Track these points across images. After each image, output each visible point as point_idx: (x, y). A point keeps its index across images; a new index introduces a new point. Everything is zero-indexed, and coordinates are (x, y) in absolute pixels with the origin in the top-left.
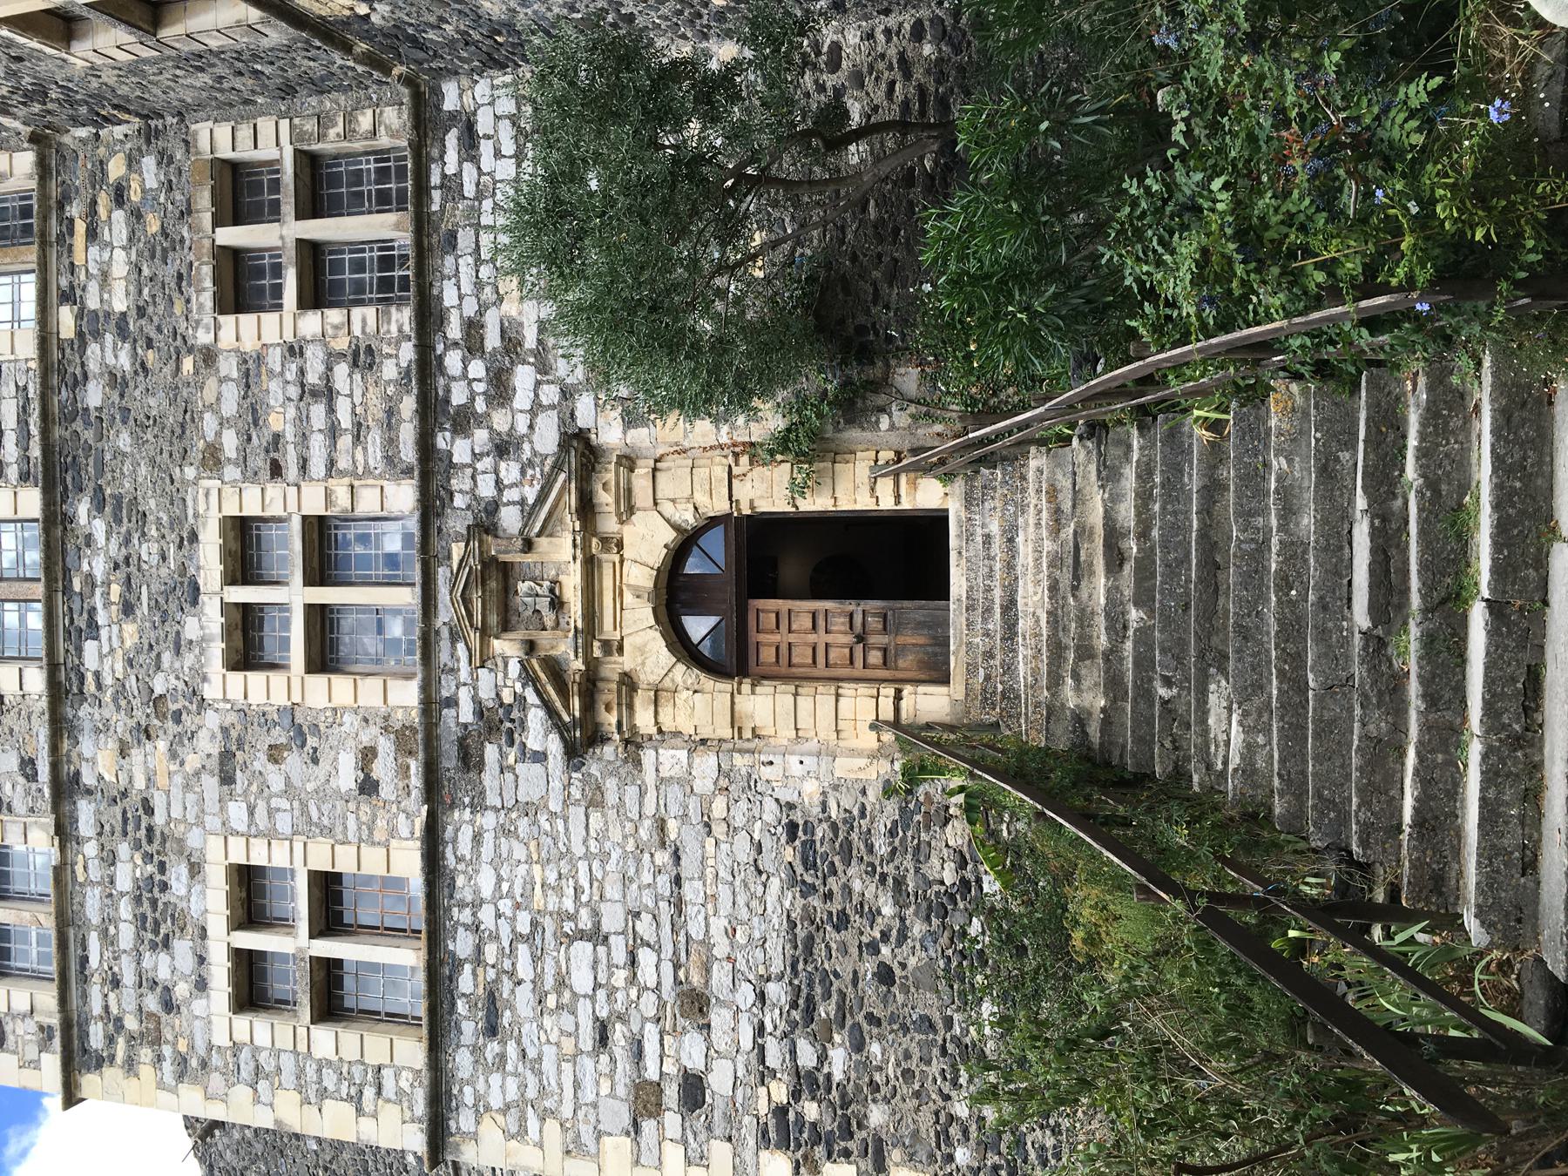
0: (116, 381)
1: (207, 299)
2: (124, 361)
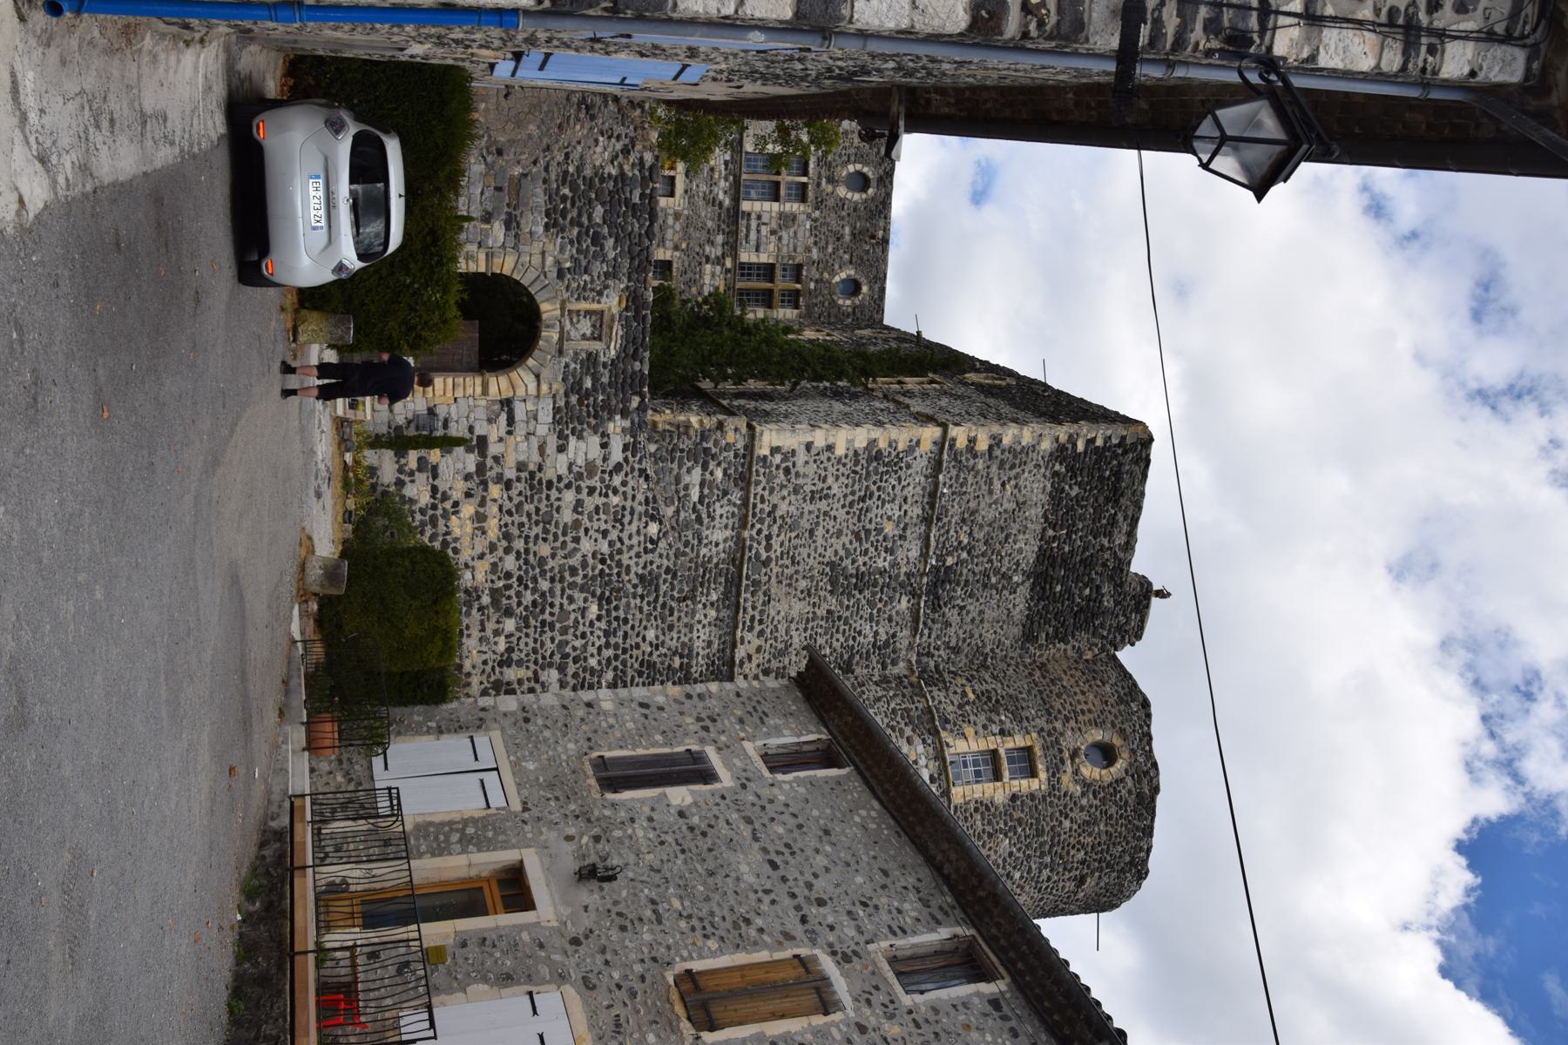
0: (712, 243)
1: (675, 265)
2: (707, 249)
